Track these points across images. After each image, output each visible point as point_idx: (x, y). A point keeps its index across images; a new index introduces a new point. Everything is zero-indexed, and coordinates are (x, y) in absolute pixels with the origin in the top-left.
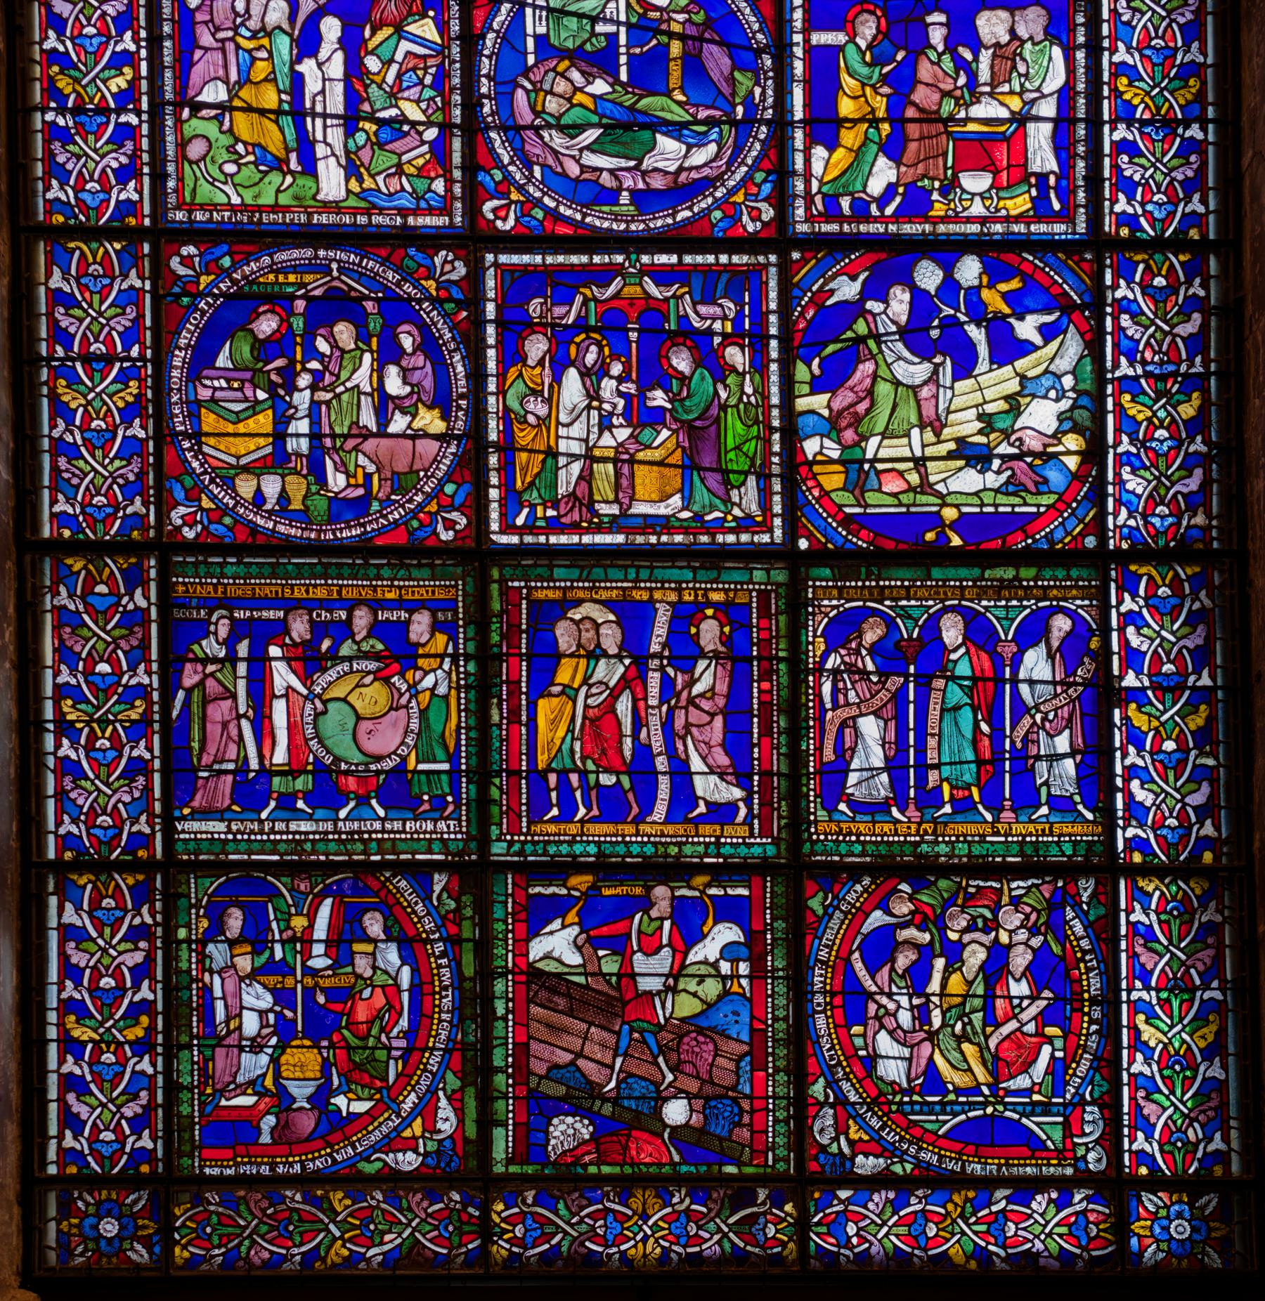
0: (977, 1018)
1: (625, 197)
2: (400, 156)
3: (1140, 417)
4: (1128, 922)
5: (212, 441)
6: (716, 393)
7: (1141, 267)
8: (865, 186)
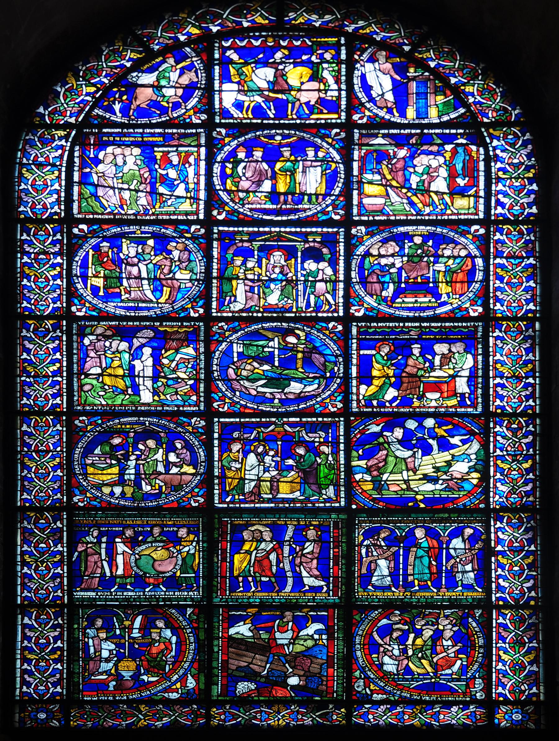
0: (428, 652)
1: (276, 401)
2: (177, 389)
3: (505, 468)
4: (496, 623)
5: (92, 476)
6: (316, 460)
7: (506, 422)
8: (383, 397)
